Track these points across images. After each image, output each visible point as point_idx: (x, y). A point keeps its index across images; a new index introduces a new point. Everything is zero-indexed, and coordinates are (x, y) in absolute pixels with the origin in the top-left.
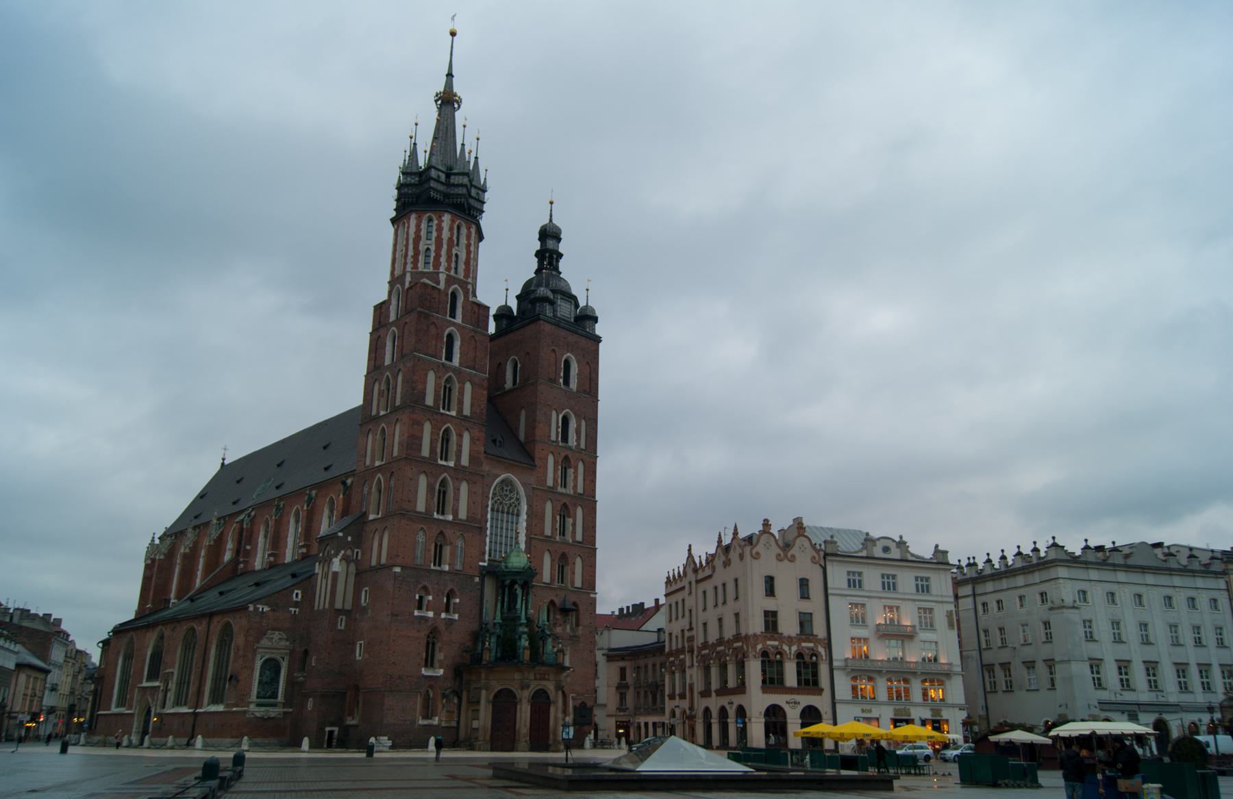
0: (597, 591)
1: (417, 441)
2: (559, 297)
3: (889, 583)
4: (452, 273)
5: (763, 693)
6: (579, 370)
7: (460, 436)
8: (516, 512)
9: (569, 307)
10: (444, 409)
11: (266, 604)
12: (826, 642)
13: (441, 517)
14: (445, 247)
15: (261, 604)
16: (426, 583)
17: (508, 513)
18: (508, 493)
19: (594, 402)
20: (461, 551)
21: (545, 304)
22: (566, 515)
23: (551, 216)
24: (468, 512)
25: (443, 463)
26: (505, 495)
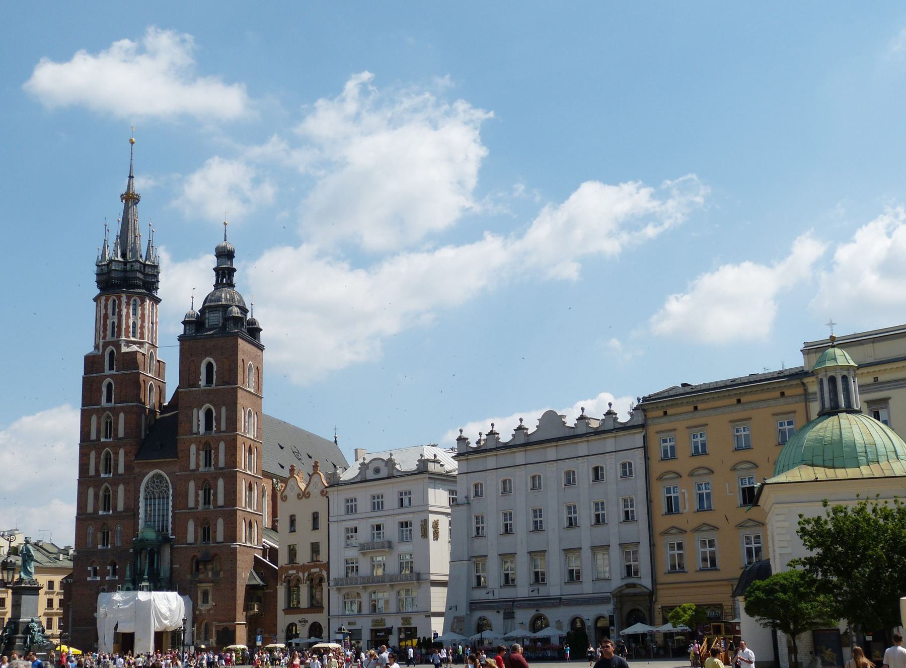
1: (86, 467)
2: (207, 311)
3: (378, 502)
4: (109, 338)
5: (285, 614)
6: (218, 367)
7: (117, 454)
10: (106, 437)
12: (327, 565)
13: (105, 513)
14: (102, 322)
16: (94, 559)
17: (159, 498)
18: (159, 484)
19: (233, 388)
23: (225, 236)
25: (107, 476)
26: (156, 485)
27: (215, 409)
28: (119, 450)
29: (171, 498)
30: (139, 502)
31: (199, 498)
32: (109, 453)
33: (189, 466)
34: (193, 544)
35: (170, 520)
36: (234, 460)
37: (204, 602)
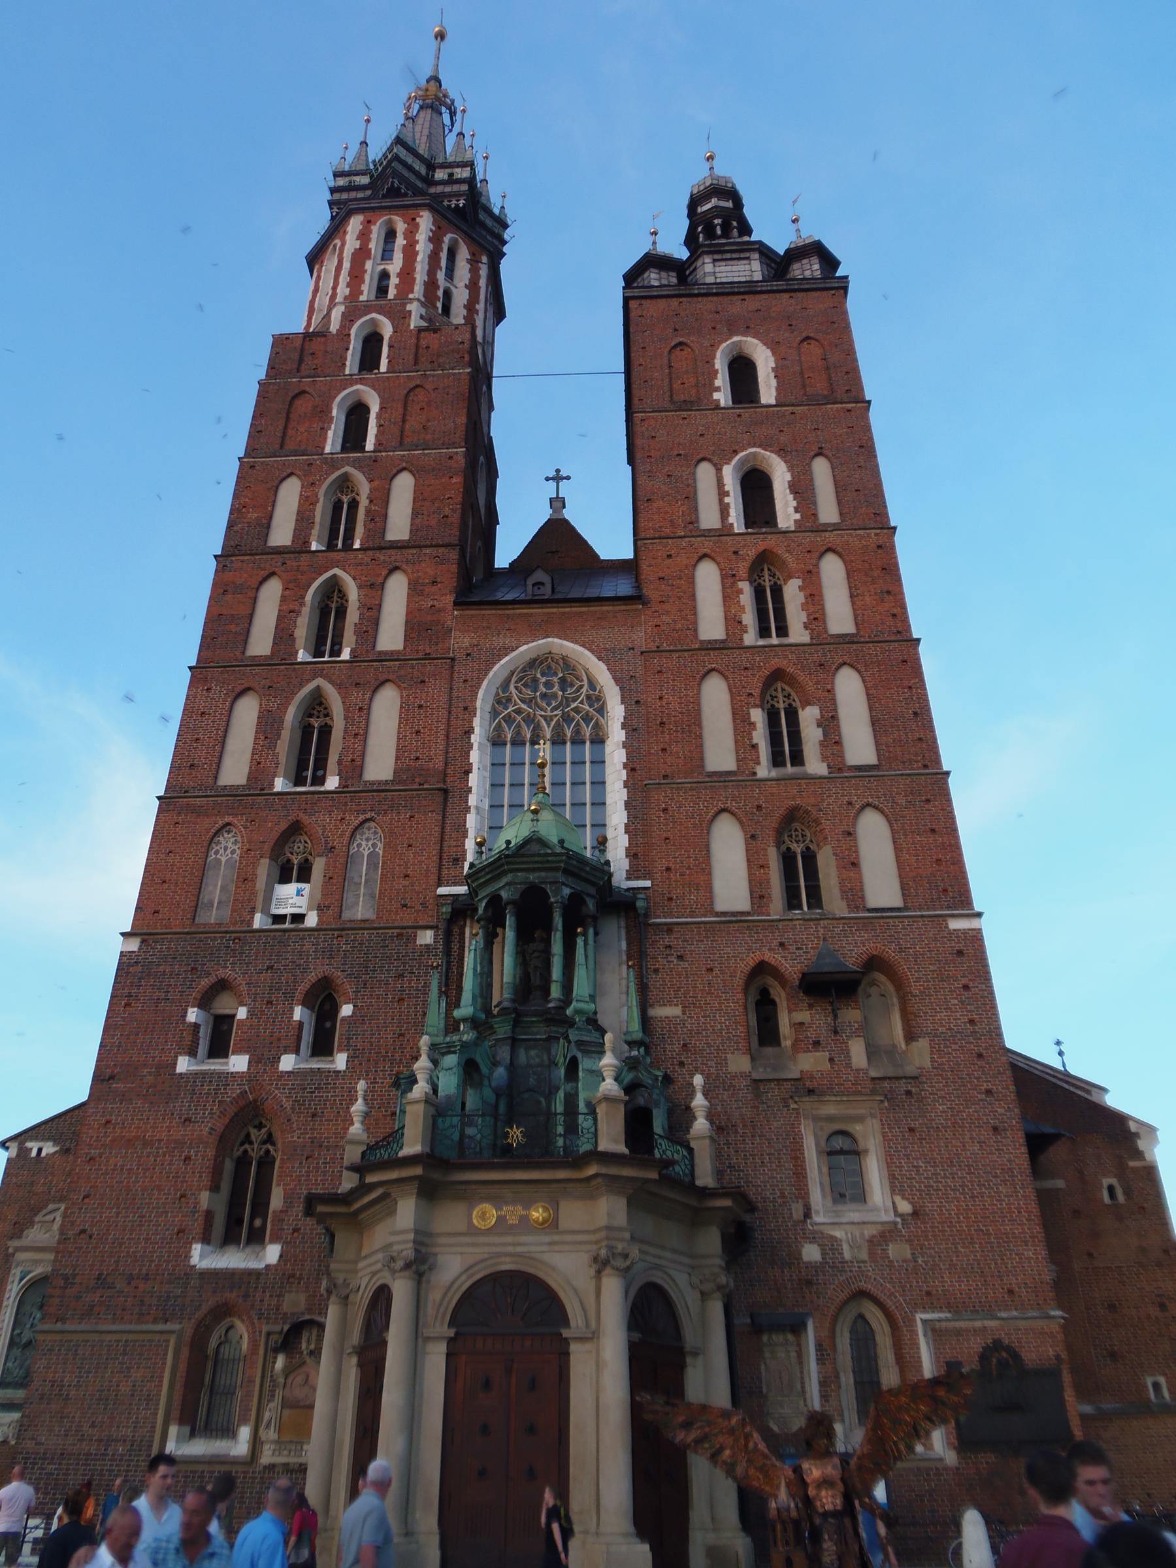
0: (977, 907)
1: (233, 628)
6: (780, 358)
7: (374, 589)
8: (587, 732)
9: (747, 267)
10: (331, 546)
11: (48, 1139)
14: (347, 265)
15: (36, 1139)
16: (226, 973)
17: (558, 741)
18: (556, 688)
19: (849, 411)
20: (372, 865)
21: (646, 275)
22: (797, 704)
24: (397, 758)
26: (544, 696)
27: (786, 462)
28: (386, 578)
29: (616, 735)
30: (471, 747)
31: (754, 733)
32: (340, 591)
33: (696, 630)
34: (748, 914)
35: (617, 817)
36: (895, 611)
37: (839, 1197)
